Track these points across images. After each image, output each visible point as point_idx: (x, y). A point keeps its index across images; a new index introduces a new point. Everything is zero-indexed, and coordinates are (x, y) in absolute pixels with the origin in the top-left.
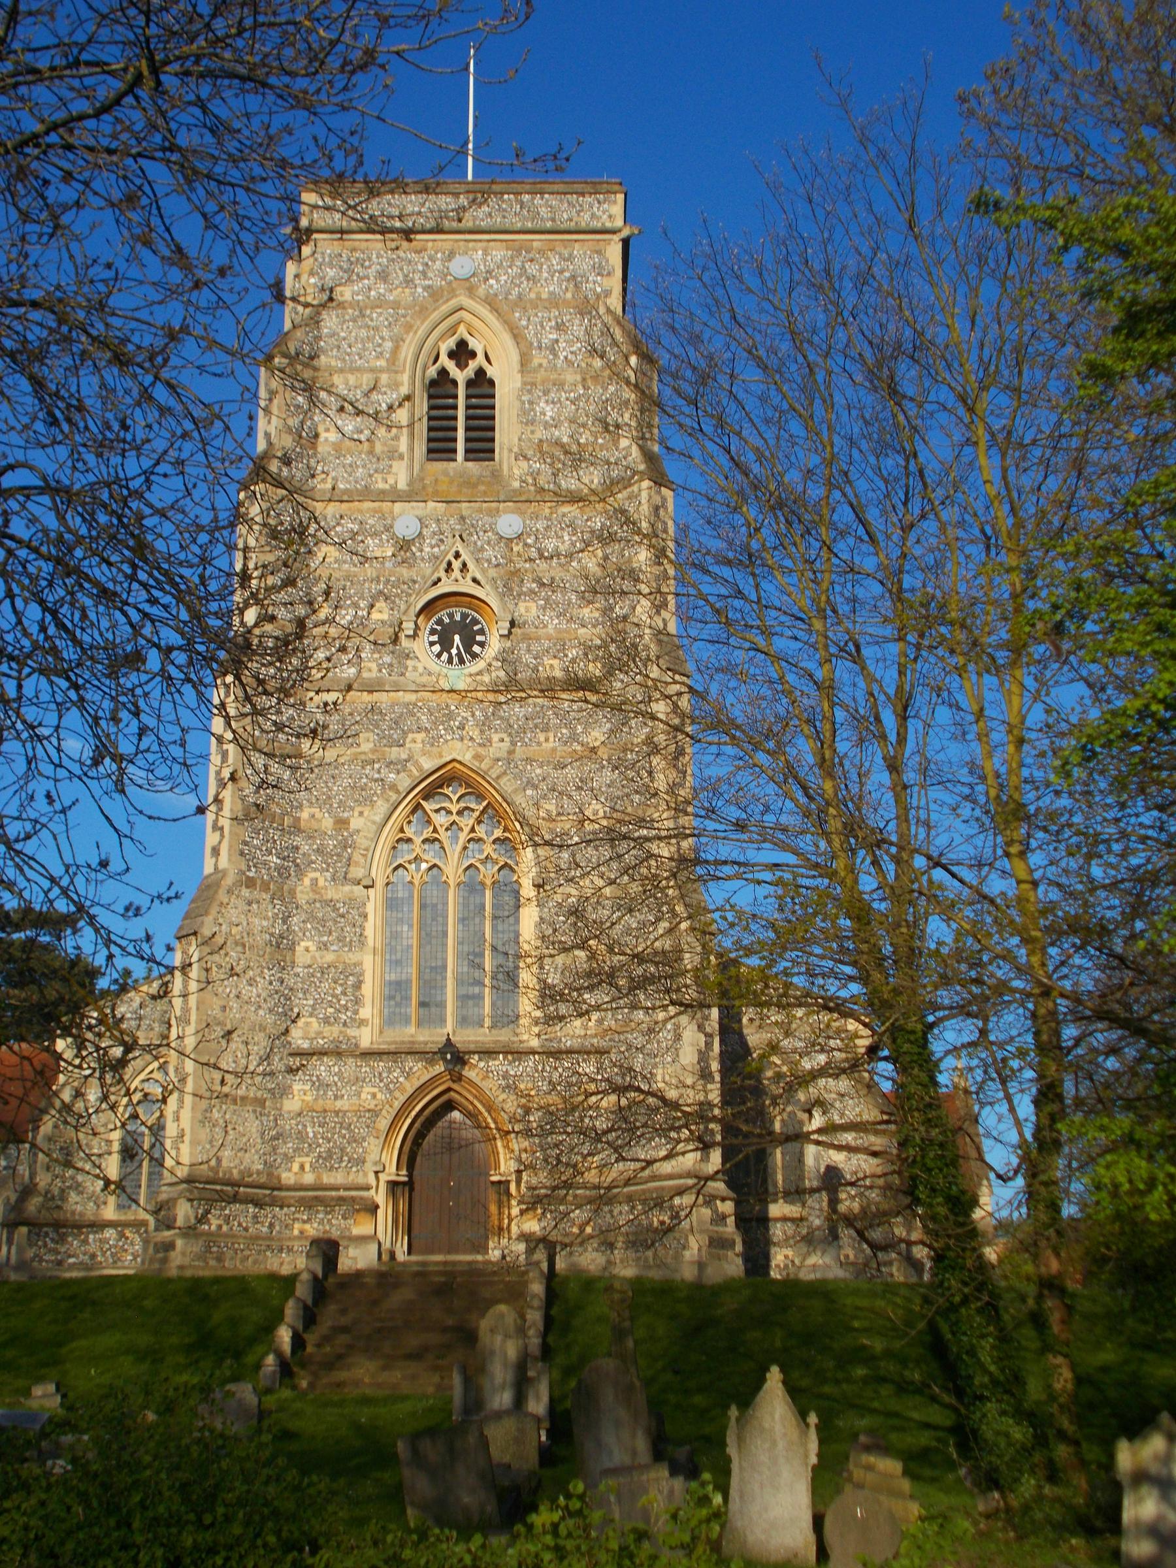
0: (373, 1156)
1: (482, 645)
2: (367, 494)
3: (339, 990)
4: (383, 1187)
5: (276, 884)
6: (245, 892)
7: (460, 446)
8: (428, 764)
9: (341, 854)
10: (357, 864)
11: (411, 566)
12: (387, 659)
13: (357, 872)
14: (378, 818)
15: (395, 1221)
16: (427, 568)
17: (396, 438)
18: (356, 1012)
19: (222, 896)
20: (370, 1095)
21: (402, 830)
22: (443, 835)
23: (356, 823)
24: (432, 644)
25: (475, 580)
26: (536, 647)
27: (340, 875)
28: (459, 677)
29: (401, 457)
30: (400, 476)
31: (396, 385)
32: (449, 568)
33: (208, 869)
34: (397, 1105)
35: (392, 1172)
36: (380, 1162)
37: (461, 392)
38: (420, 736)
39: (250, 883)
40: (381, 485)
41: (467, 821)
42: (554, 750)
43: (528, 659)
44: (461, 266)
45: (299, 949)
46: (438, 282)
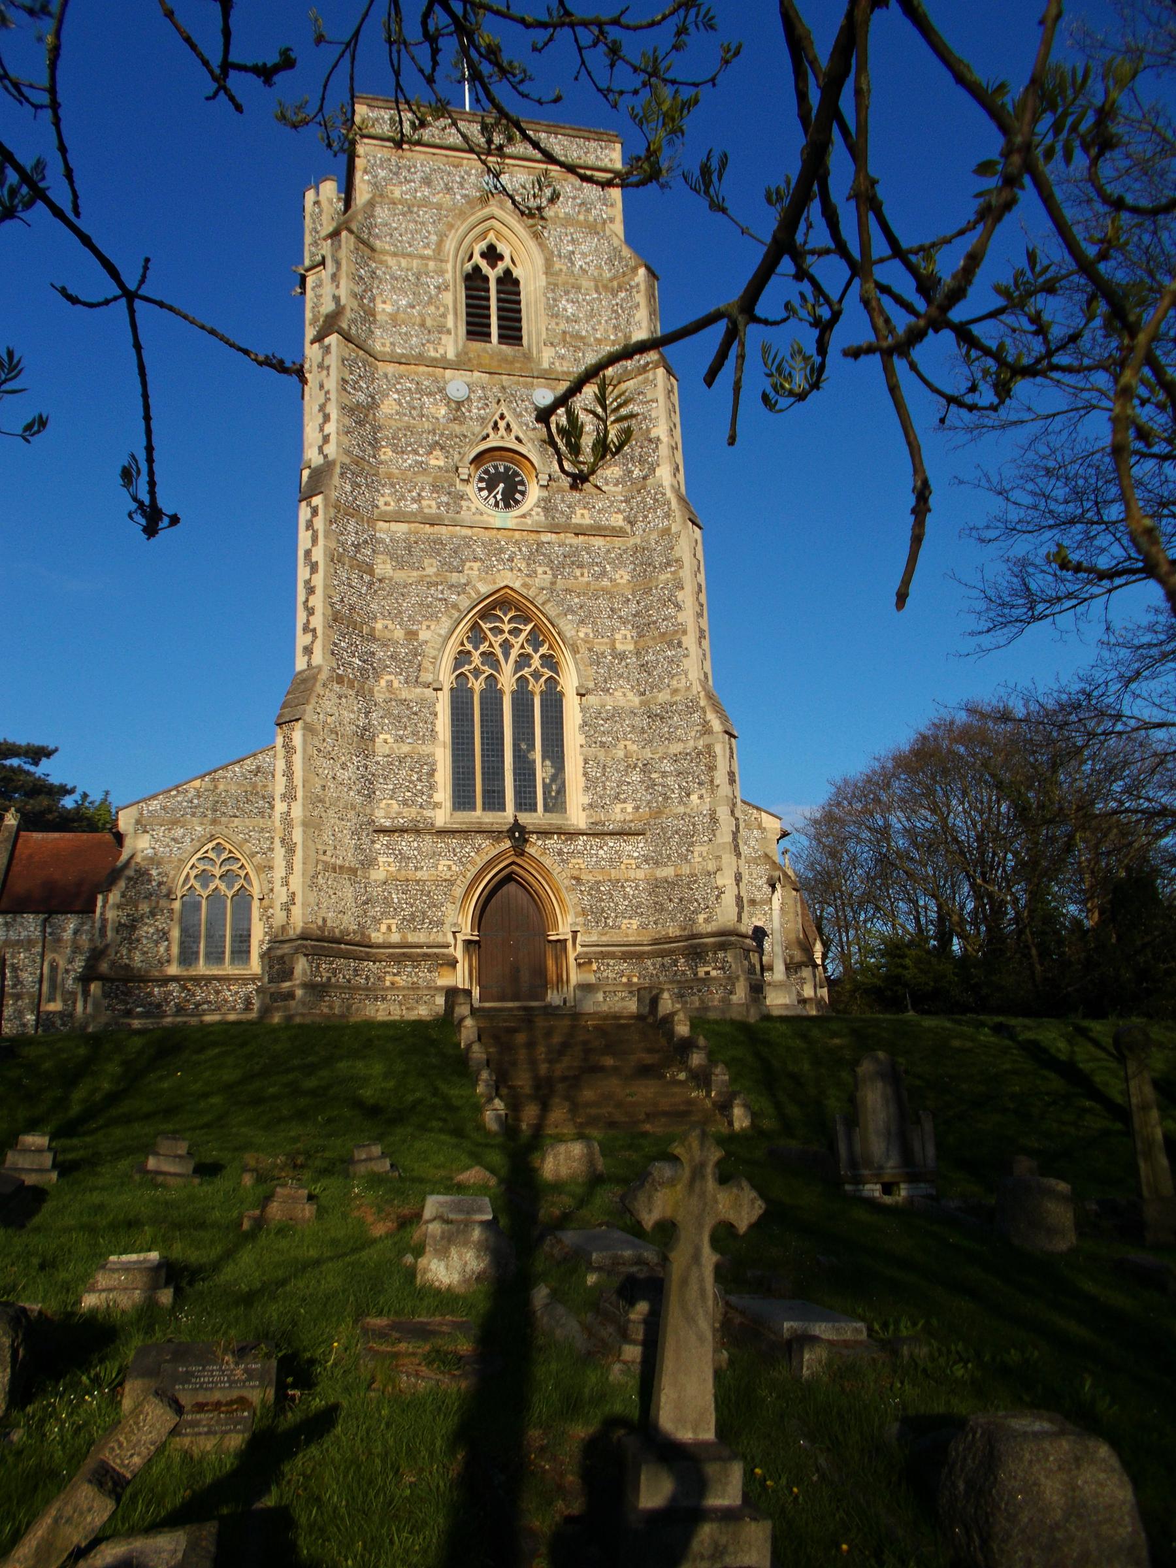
2: (420, 359)
14: (443, 632)
29: (449, 332)
40: (432, 354)
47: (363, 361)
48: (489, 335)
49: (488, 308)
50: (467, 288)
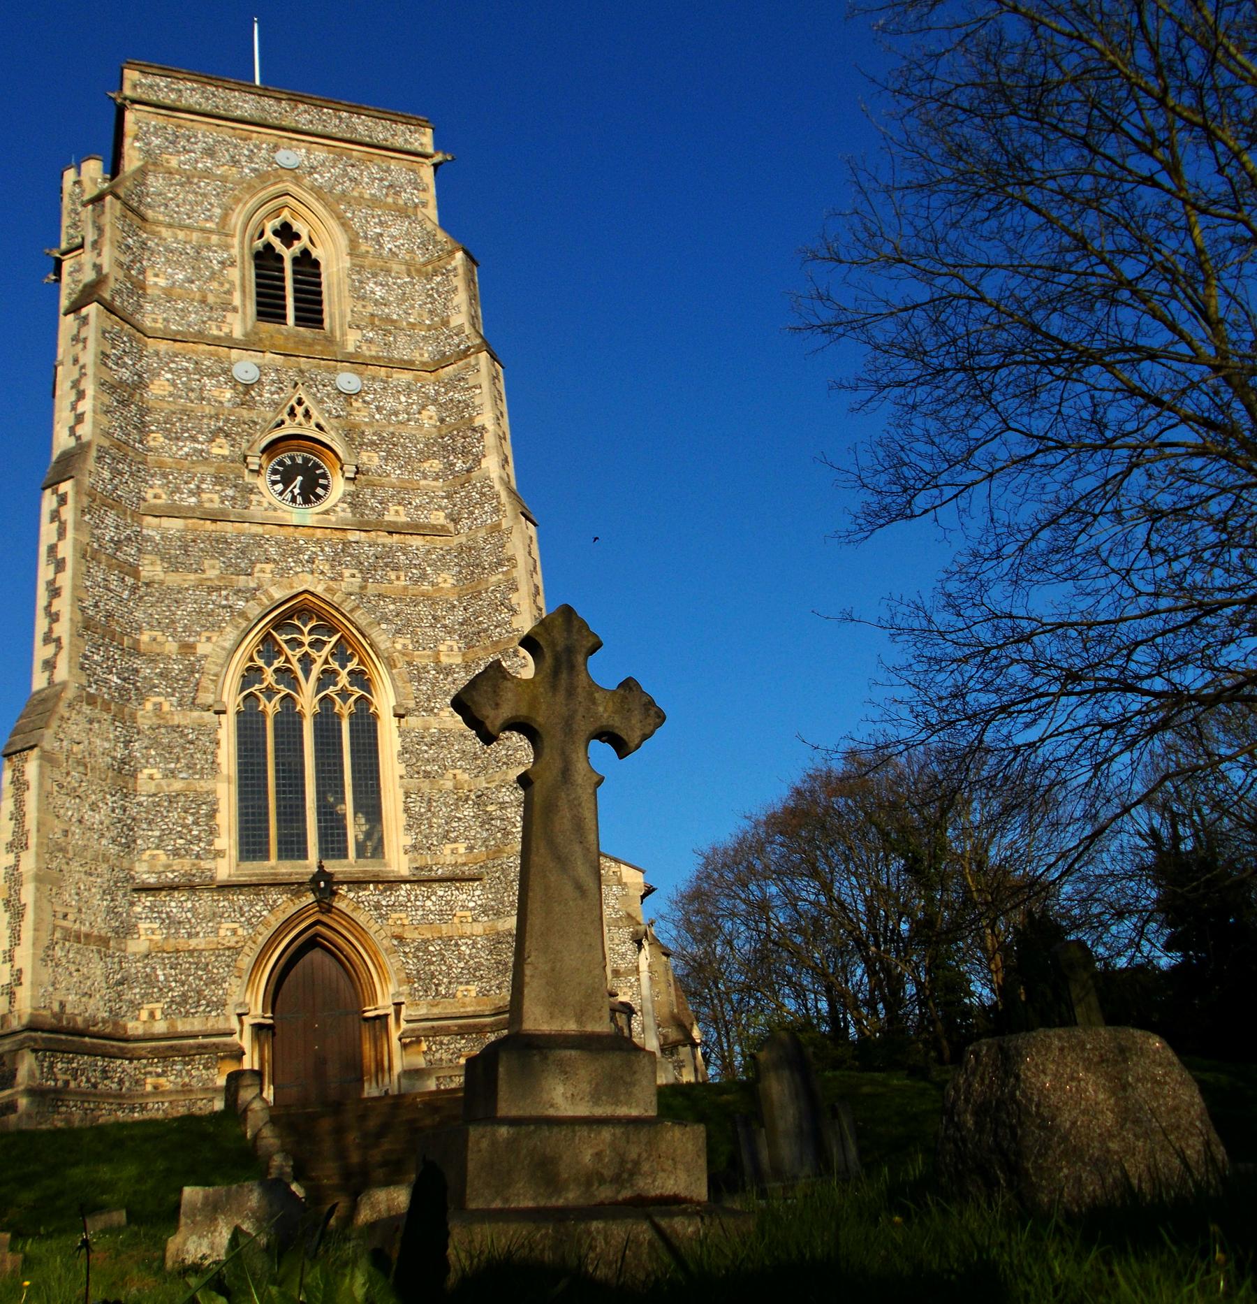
0: (232, 1000)
1: (325, 488)
2: (200, 337)
3: (190, 819)
4: (247, 1031)
5: (118, 705)
6: (86, 709)
8: (278, 594)
10: (206, 690)
11: (251, 408)
12: (230, 492)
13: (206, 698)
17: (229, 292)
18: (211, 843)
19: (62, 710)
21: (251, 659)
22: (297, 667)
23: (202, 648)
24: (274, 483)
25: (318, 426)
26: (380, 493)
27: (188, 700)
28: (307, 515)
29: (235, 310)
31: (227, 247)
32: (292, 413)
33: (39, 681)
34: (261, 940)
35: (257, 1012)
36: (245, 1002)
39: (91, 699)
40: (215, 332)
42: (405, 588)
43: (372, 502)
47: (128, 335)
48: (284, 317)
49: (283, 288)
50: (257, 267)
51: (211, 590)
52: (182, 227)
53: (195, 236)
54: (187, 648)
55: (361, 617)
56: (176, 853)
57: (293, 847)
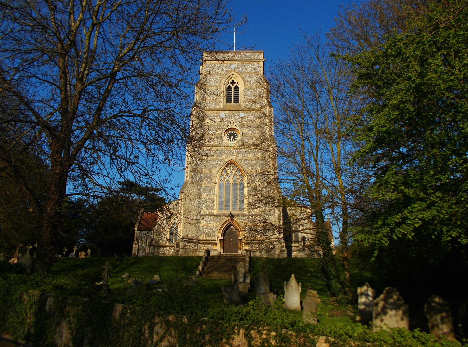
0: (216, 235)
2: (215, 109)
5: (198, 183)
6: (192, 185)
7: (233, 100)
8: (226, 160)
9: (210, 178)
13: (213, 181)
15: (221, 247)
16: (226, 123)
19: (188, 185)
20: (216, 223)
22: (229, 174)
23: (213, 172)
28: (232, 144)
30: (221, 106)
31: (221, 89)
32: (231, 123)
33: (185, 180)
34: (221, 225)
35: (220, 237)
36: (218, 236)
37: (233, 90)
38: (225, 155)
39: (193, 183)
41: (234, 171)
43: (246, 140)
44: (233, 66)
45: (202, 195)
46: (228, 70)
51: (215, 160)
52: (212, 86)
53: (215, 87)
54: (210, 172)
55: (242, 164)
56: (208, 209)
57: (227, 206)
